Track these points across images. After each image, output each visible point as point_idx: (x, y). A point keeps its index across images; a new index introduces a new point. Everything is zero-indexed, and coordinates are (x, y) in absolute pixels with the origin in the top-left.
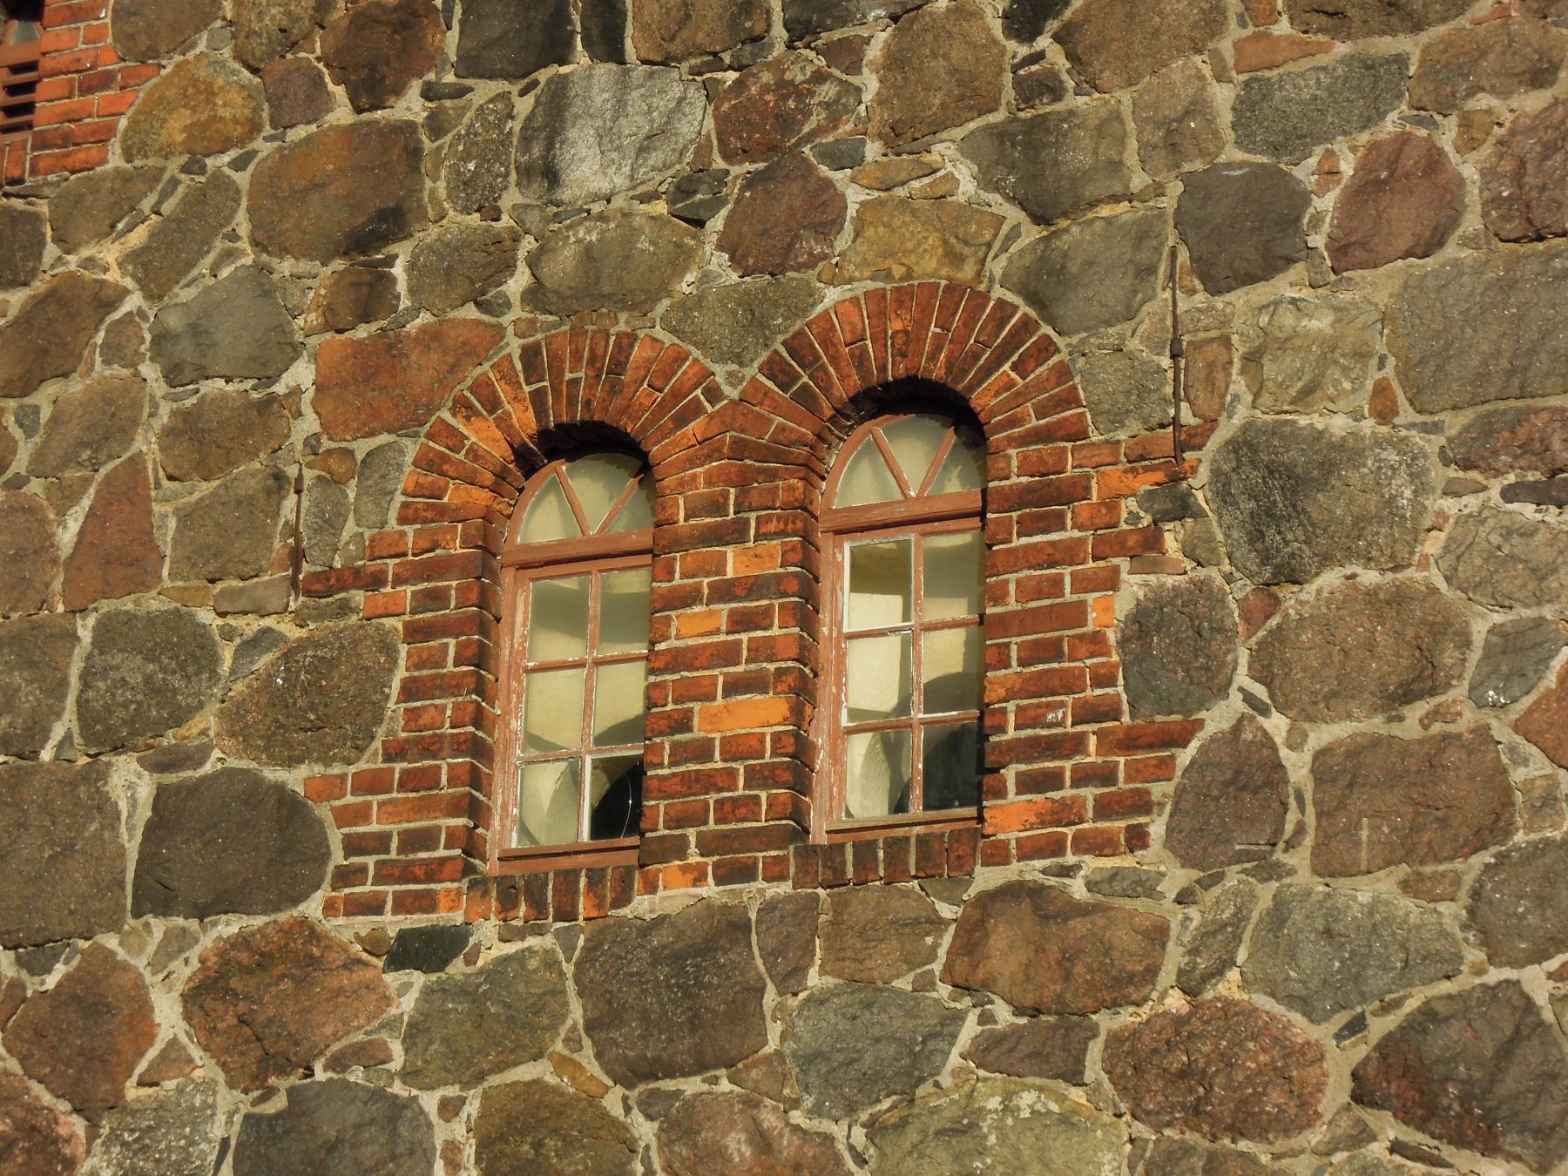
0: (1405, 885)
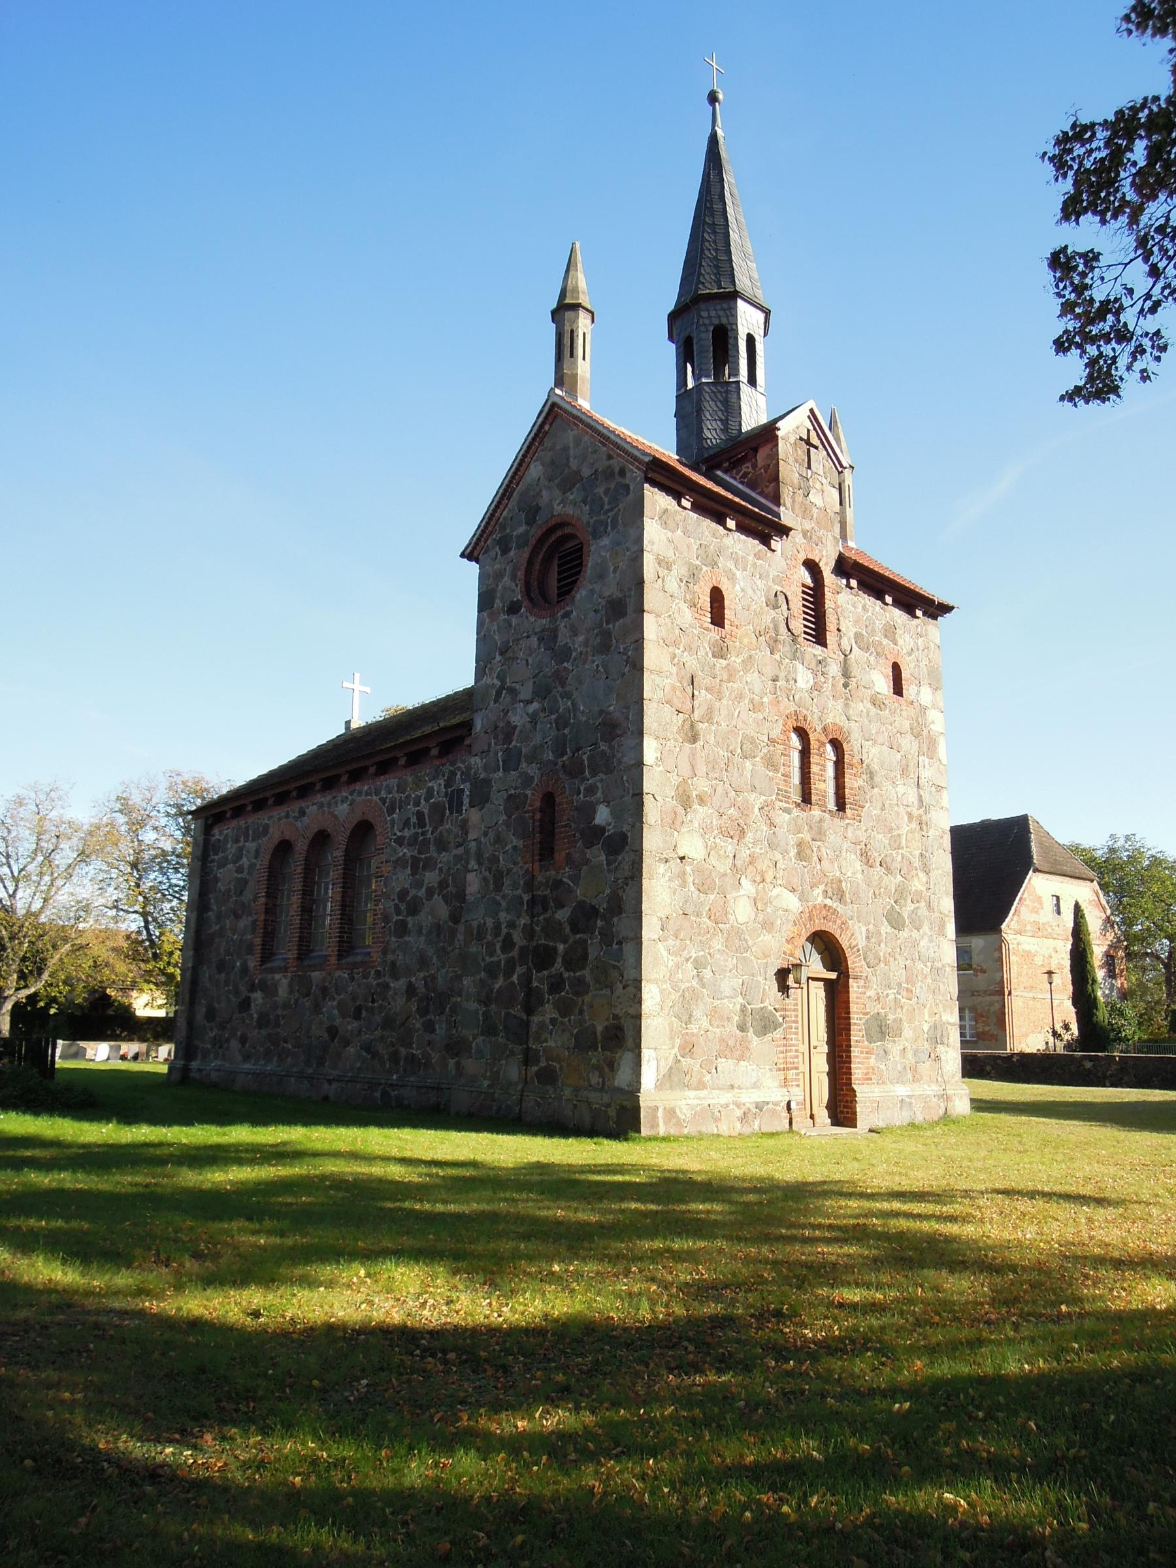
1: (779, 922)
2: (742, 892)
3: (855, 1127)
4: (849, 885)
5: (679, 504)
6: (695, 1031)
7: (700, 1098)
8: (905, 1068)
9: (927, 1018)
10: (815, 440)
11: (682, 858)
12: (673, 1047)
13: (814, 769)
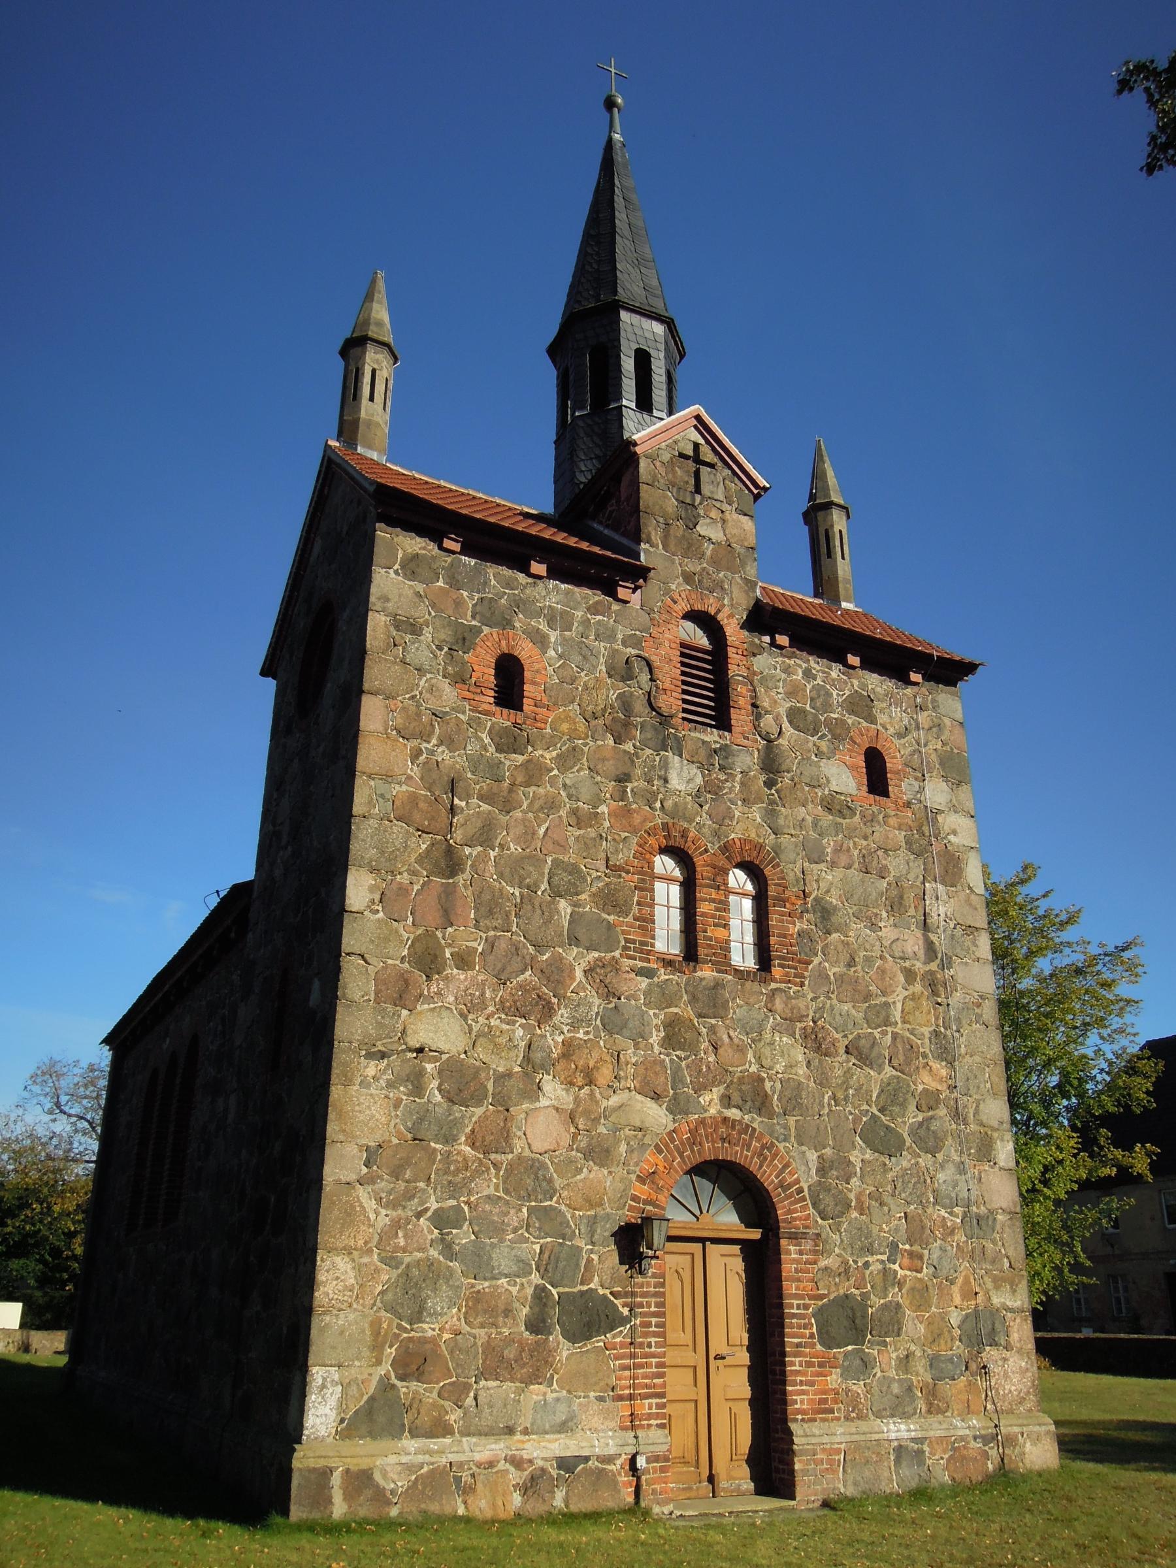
0: (853, 1007)
1: (623, 1147)
2: (544, 1102)
3: (793, 1498)
4: (778, 1086)
5: (441, 548)
6: (430, 1333)
7: (431, 1453)
8: (910, 1389)
9: (957, 1300)
10: (707, 455)
11: (420, 1050)
12: (379, 1362)
13: (704, 908)
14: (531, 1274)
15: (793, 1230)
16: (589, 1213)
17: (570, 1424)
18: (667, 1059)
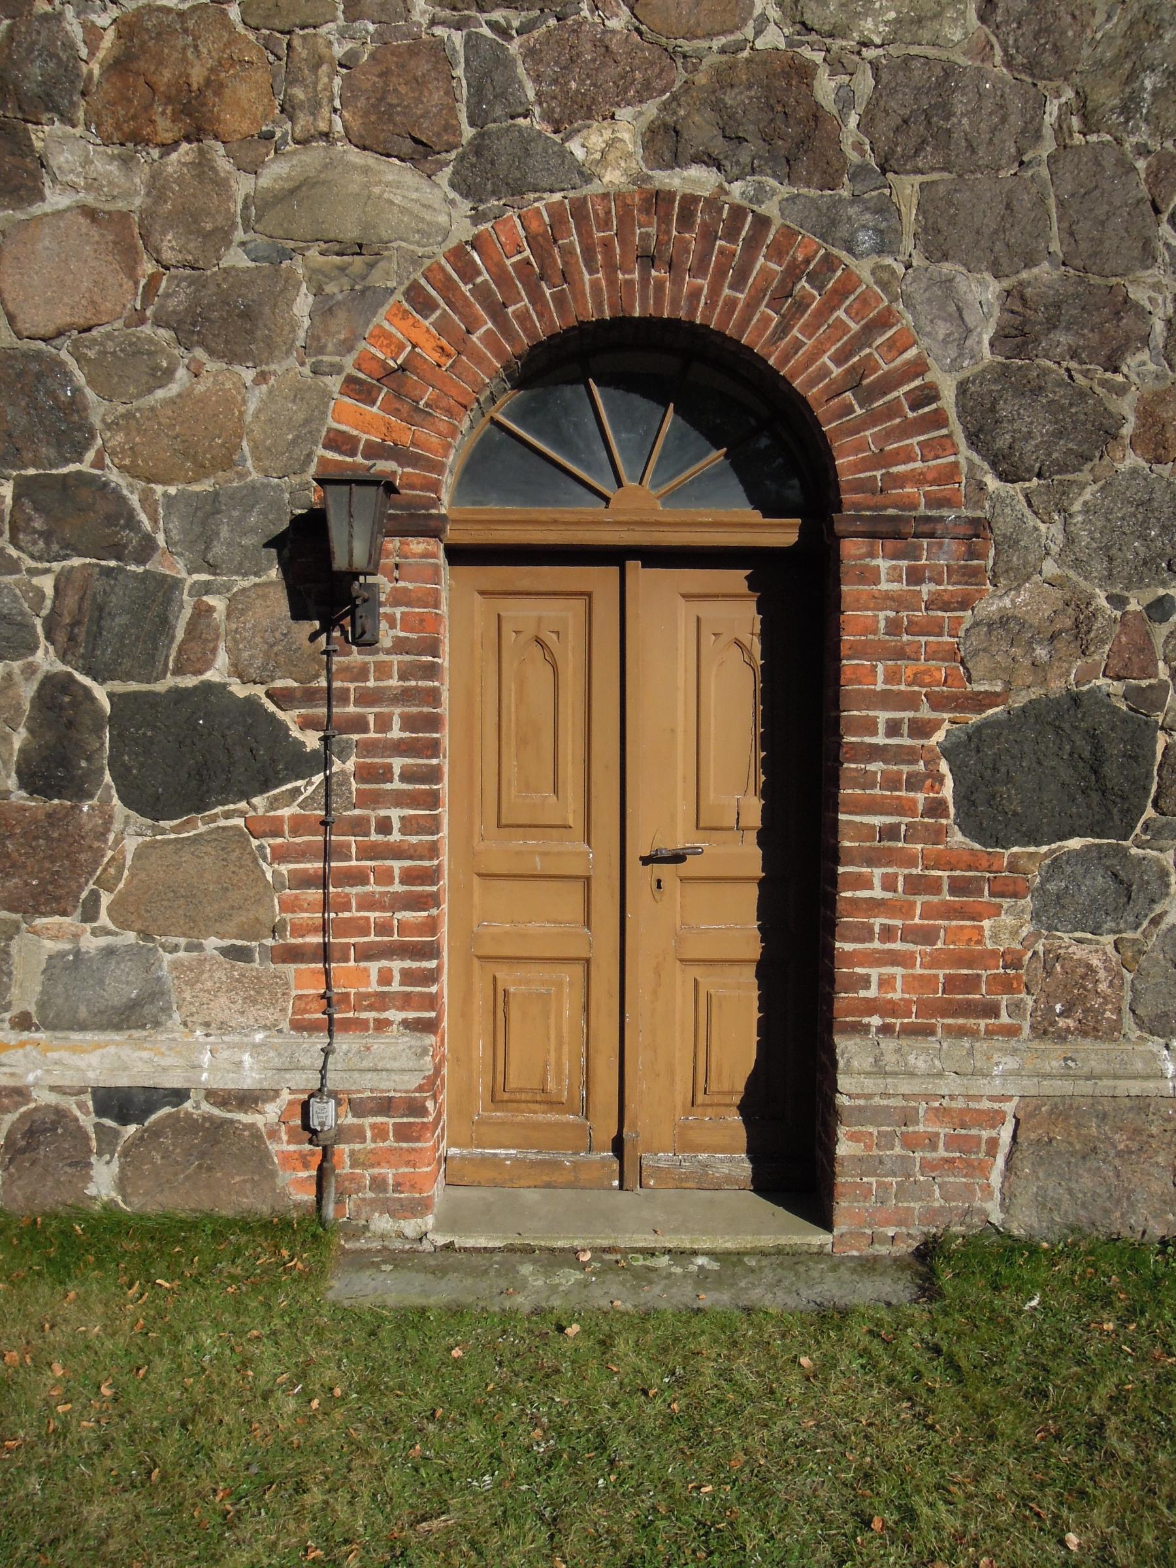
1: (303, 304)
2: (56, 200)
4: (865, 83)
14: (33, 649)
15: (891, 512)
16: (196, 488)
17: (148, 1010)
18: (458, 38)
